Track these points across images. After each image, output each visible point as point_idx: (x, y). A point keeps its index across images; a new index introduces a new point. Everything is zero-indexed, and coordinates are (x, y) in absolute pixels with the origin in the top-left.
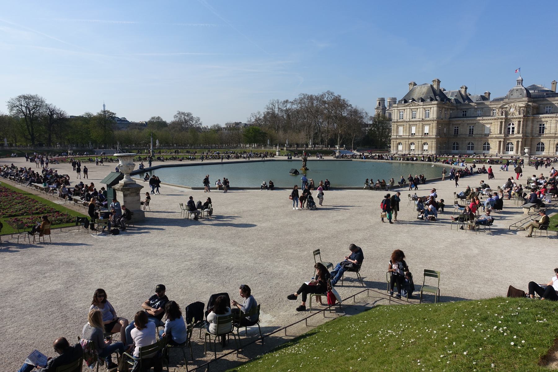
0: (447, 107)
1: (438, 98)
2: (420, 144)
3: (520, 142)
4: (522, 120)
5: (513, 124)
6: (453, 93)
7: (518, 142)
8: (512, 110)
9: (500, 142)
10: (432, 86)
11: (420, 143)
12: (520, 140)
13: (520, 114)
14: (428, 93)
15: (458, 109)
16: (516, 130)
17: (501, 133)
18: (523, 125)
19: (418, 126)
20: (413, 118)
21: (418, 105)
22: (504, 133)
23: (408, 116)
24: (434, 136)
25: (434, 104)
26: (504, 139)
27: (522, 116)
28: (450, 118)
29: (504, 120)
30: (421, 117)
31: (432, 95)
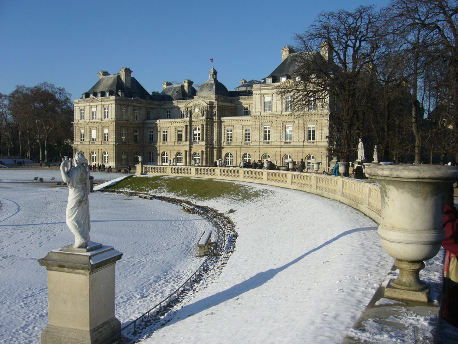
0: (139, 105)
1: (120, 93)
2: (100, 154)
3: (204, 153)
4: (204, 124)
5: (199, 130)
6: (175, 88)
7: (202, 152)
8: (197, 111)
9: (186, 151)
10: (119, 77)
11: (100, 151)
12: (204, 149)
13: (203, 116)
14: (112, 85)
15: (161, 109)
16: (201, 136)
17: (186, 140)
18: (207, 130)
19: (98, 129)
20: (93, 118)
21: (97, 101)
22: (190, 140)
23: (88, 115)
24: (112, 143)
25: (112, 100)
26: (190, 148)
27: (204, 118)
28: (145, 120)
29: (188, 124)
30: (100, 117)
31: (114, 89)
